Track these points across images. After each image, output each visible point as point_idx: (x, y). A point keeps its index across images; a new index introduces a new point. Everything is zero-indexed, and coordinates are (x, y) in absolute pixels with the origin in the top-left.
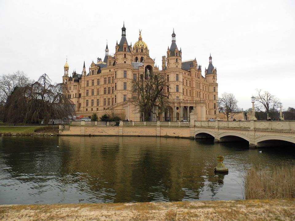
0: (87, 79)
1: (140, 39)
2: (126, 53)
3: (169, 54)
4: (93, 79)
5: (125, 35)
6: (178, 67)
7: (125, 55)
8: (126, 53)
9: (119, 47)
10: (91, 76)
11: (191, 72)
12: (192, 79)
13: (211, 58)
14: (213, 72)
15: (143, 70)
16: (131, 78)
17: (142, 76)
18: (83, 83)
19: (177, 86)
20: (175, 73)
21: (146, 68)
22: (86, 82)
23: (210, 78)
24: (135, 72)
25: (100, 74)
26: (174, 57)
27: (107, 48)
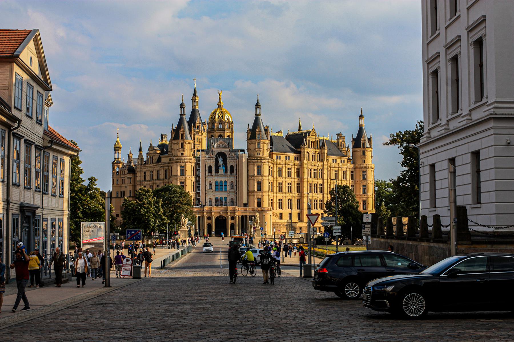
0: (145, 170)
1: (219, 106)
2: (183, 141)
3: (250, 135)
4: (151, 169)
7: (182, 144)
8: (183, 141)
10: (148, 165)
12: (301, 165)
13: (361, 116)
14: (362, 144)
17: (210, 168)
18: (140, 176)
19: (259, 182)
20: (255, 163)
21: (216, 156)
22: (143, 174)
25: (160, 163)
26: (254, 141)
27: (195, 94)
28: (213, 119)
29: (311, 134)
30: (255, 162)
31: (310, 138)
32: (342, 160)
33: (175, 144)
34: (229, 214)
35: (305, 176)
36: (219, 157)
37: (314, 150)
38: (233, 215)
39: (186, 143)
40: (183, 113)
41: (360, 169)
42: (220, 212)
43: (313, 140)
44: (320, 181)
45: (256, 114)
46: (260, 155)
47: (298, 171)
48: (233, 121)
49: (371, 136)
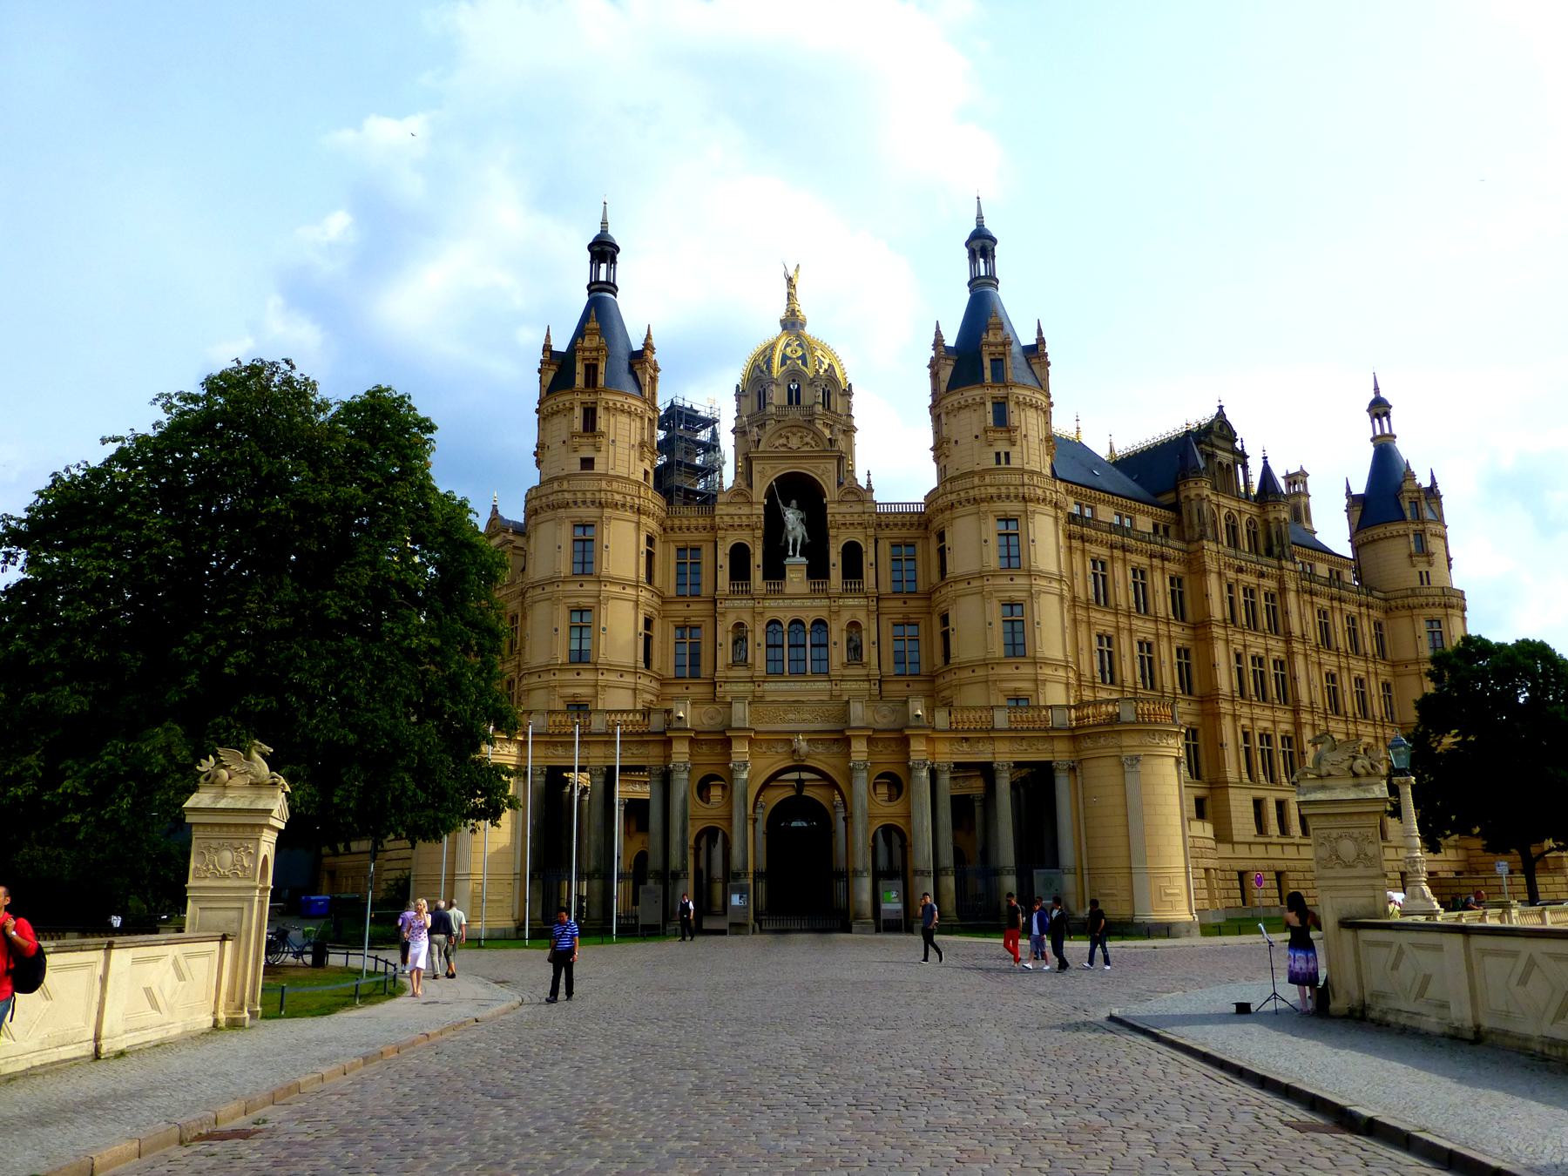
1: (792, 323)
2: (592, 398)
3: (946, 373)
5: (611, 287)
6: (1015, 463)
7: (590, 416)
8: (592, 398)
9: (560, 367)
11: (1184, 512)
13: (1379, 408)
14: (1406, 505)
15: (745, 510)
16: (632, 575)
17: (740, 555)
20: (984, 506)
21: (770, 495)
23: (1394, 554)
24: (687, 536)
26: (973, 393)
28: (762, 371)
29: (1216, 427)
30: (982, 500)
31: (1212, 445)
32: (1331, 571)
33: (553, 414)
34: (859, 750)
35: (1217, 609)
36: (787, 505)
37: (1234, 504)
38: (887, 760)
39: (607, 409)
40: (603, 278)
41: (1416, 611)
42: (790, 741)
43: (1224, 457)
44: (1277, 648)
45: (969, 284)
46: (1008, 462)
47: (1176, 588)
48: (849, 380)
49: (1433, 477)
